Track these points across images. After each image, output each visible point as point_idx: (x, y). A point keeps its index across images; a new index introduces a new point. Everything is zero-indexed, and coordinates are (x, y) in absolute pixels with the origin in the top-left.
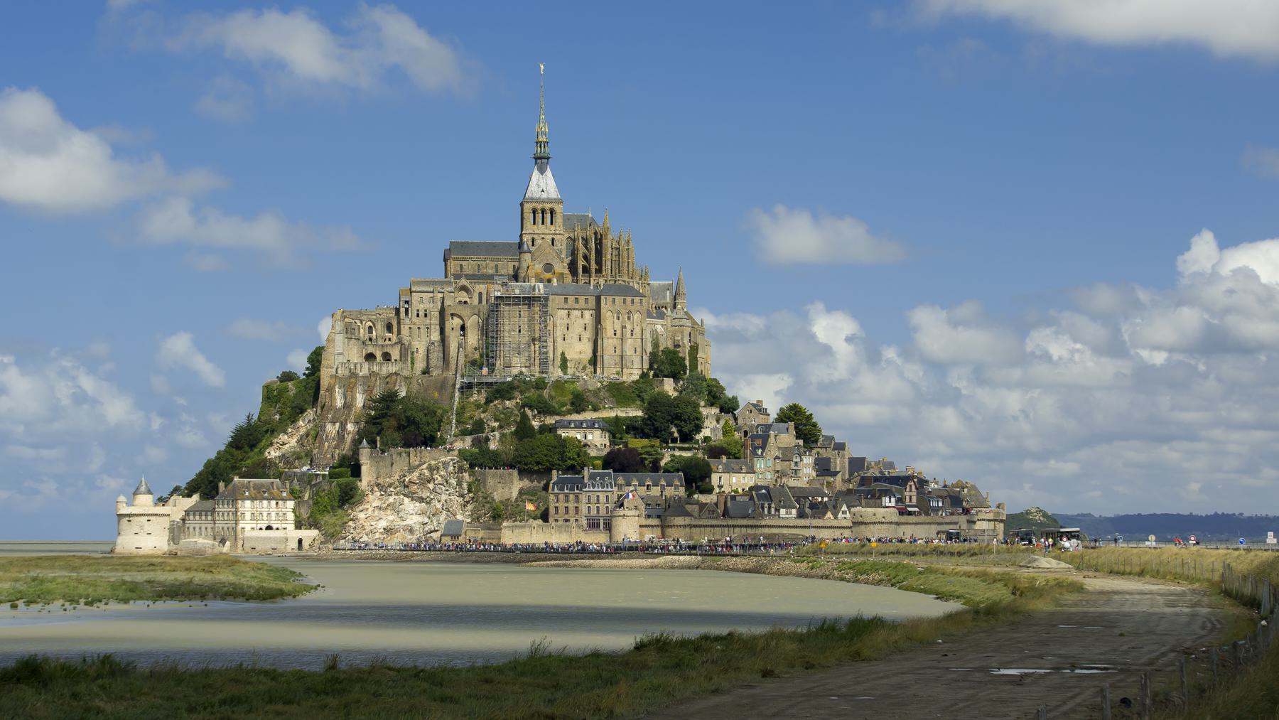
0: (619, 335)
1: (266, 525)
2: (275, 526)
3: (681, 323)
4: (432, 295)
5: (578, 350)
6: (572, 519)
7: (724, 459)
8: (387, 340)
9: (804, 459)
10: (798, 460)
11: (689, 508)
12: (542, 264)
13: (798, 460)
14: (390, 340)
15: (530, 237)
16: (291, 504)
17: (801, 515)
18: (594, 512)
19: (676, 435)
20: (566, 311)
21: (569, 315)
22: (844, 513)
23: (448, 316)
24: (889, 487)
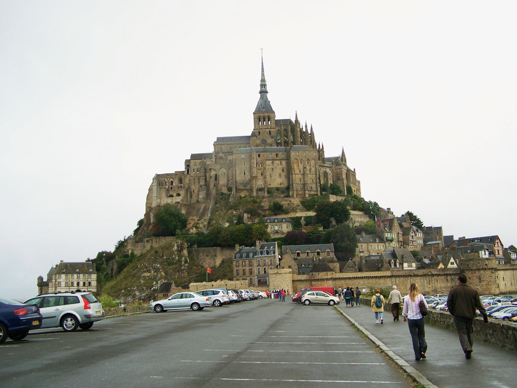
0: (302, 173)
1: (76, 290)
2: (83, 290)
3: (340, 167)
4: (200, 161)
5: (279, 183)
6: (248, 278)
9: (418, 234)
11: (331, 265)
12: (260, 140)
13: (413, 234)
14: (181, 187)
16: (94, 276)
17: (418, 268)
18: (262, 272)
19: (334, 223)
20: (271, 161)
21: (273, 163)
22: (452, 263)
23: (208, 170)
24: (482, 244)
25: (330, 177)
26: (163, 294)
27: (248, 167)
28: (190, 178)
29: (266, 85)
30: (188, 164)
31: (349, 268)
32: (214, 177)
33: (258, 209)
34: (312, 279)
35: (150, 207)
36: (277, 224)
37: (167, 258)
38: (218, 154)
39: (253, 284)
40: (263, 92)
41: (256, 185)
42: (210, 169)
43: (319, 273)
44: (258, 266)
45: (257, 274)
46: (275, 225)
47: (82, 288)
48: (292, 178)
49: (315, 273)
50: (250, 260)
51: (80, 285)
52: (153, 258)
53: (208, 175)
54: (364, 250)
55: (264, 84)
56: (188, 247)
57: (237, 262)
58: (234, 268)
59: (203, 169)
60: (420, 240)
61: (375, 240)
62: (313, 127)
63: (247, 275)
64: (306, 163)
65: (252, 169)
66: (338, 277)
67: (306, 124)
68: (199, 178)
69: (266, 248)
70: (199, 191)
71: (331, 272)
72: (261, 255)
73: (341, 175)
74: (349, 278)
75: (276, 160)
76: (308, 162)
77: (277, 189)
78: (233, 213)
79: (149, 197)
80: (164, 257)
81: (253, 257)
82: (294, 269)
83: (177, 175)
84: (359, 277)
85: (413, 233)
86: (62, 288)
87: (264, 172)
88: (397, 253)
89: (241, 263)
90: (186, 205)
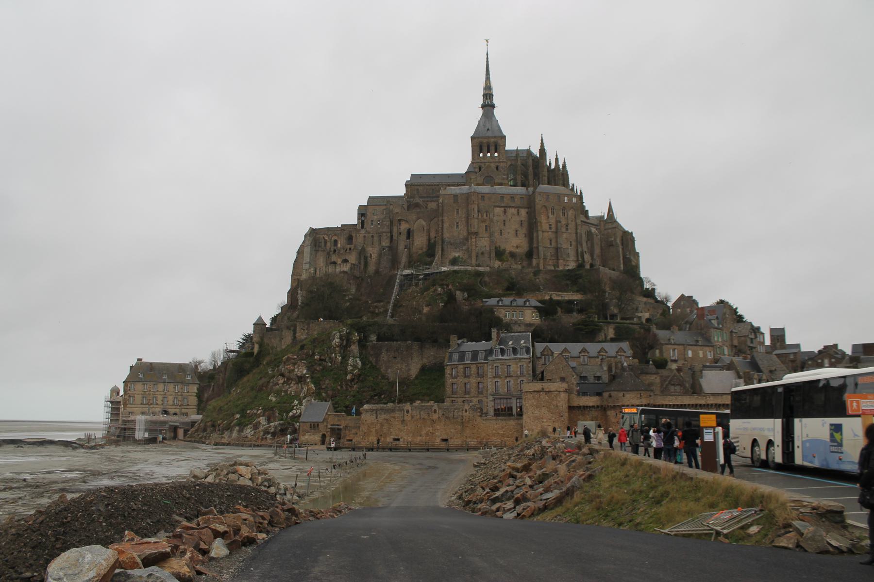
0: (553, 229)
2: (172, 411)
3: (614, 226)
4: (384, 207)
5: (515, 245)
6: (475, 400)
7: (675, 328)
8: (348, 249)
9: (758, 336)
10: (753, 336)
13: (753, 336)
14: (350, 249)
15: (476, 166)
16: (194, 389)
20: (503, 209)
21: (505, 212)
25: (597, 240)
26: (309, 424)
27: (464, 216)
28: (366, 235)
29: (493, 95)
30: (362, 212)
31: (673, 387)
32: (406, 233)
33: (480, 286)
34: (610, 404)
35: (298, 279)
36: (516, 310)
37: (321, 360)
38: (412, 199)
39: (484, 411)
40: (488, 106)
41: (476, 247)
42: (400, 220)
43: (625, 393)
44: (494, 377)
45: (493, 392)
46: (513, 310)
47: (171, 408)
48: (538, 236)
49: (616, 393)
50: (479, 365)
51: (169, 402)
52: (296, 357)
53: (397, 230)
54: (678, 357)
55: (490, 92)
56: (360, 341)
57: (452, 369)
58: (448, 380)
59: (388, 221)
60: (761, 346)
61: (697, 341)
62: (566, 163)
63: (472, 394)
64: (561, 215)
65: (469, 221)
66: (661, 404)
67: (557, 156)
68: (381, 234)
69: (510, 343)
70: (380, 256)
71: (649, 393)
72: (502, 356)
73: (615, 239)
74: (681, 405)
75: (510, 207)
76: (564, 213)
77: (513, 255)
78: (437, 290)
79: (297, 265)
80: (316, 357)
81: (486, 359)
82: (572, 385)
83: (344, 230)
84: (701, 405)
85: (753, 334)
86: (136, 406)
87: (490, 227)
88: (760, 363)
89: (462, 370)
90: (358, 278)
